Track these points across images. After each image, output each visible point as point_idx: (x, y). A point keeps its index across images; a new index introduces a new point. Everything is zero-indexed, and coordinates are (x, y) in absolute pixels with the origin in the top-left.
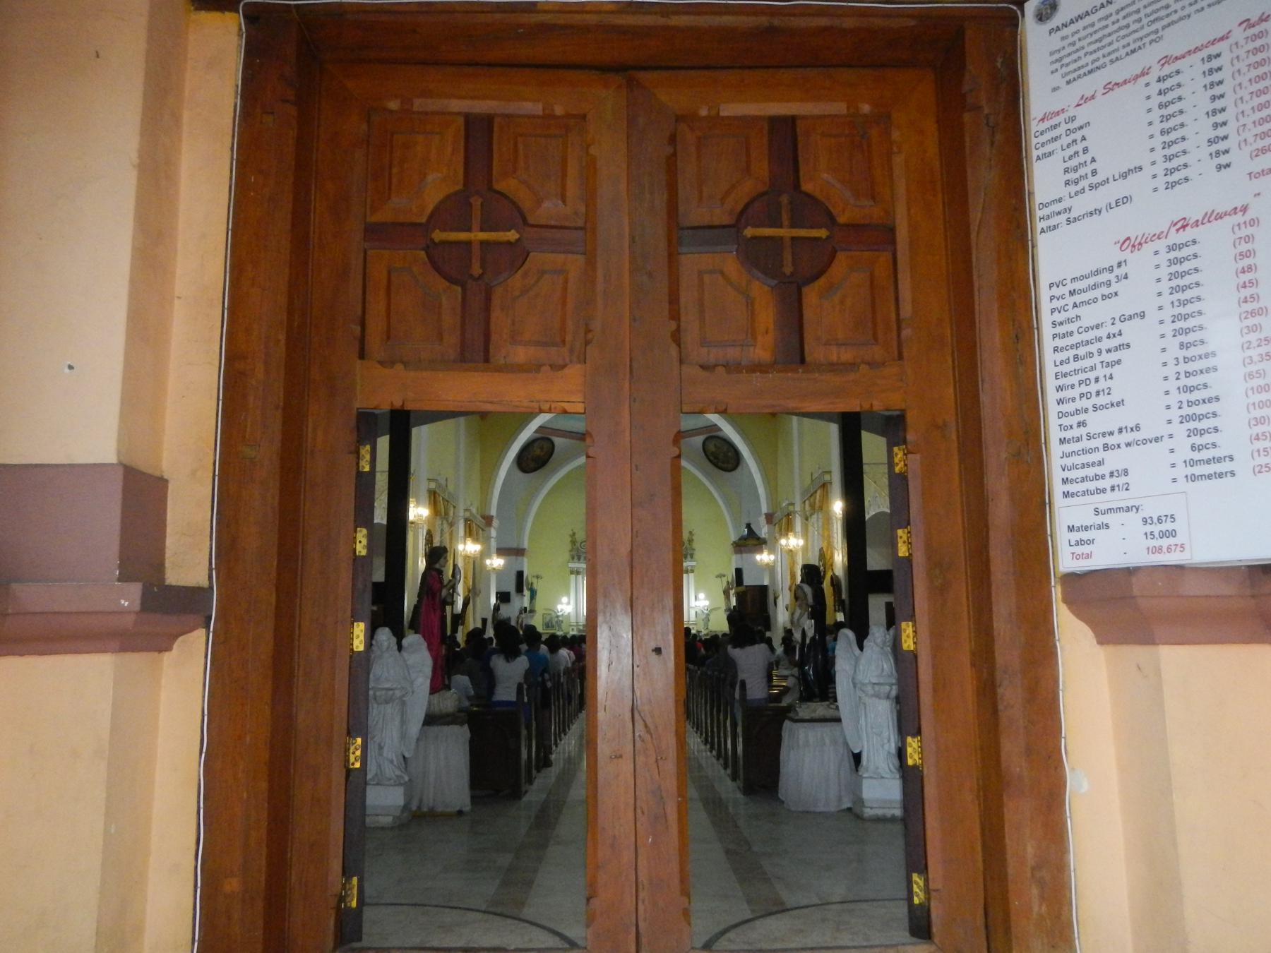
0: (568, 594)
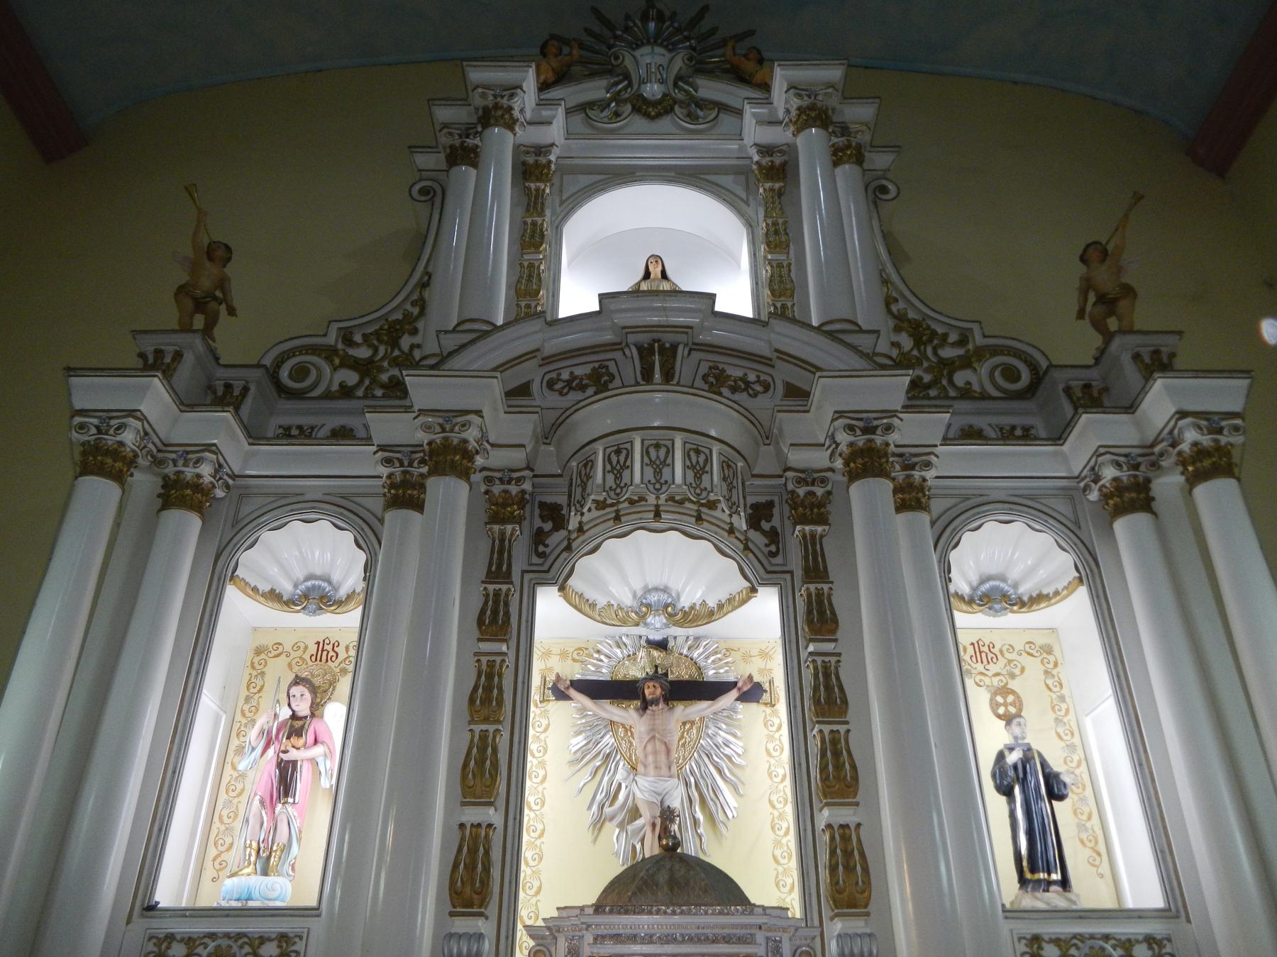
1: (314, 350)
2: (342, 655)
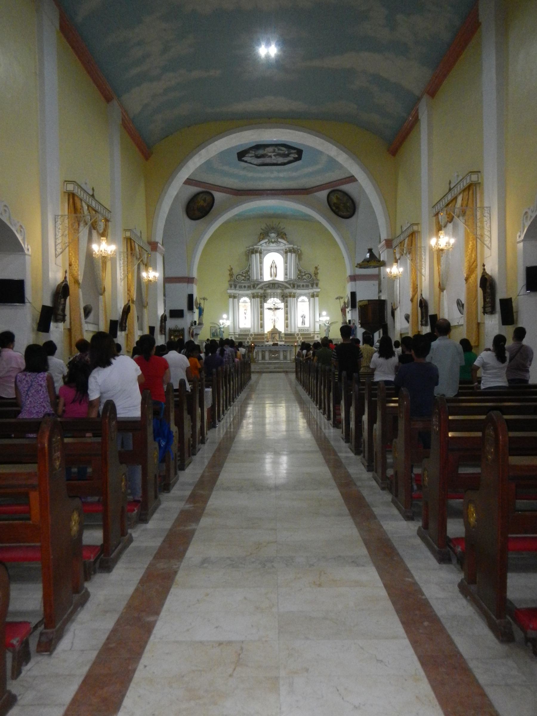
0: (228, 313)
1: (240, 275)
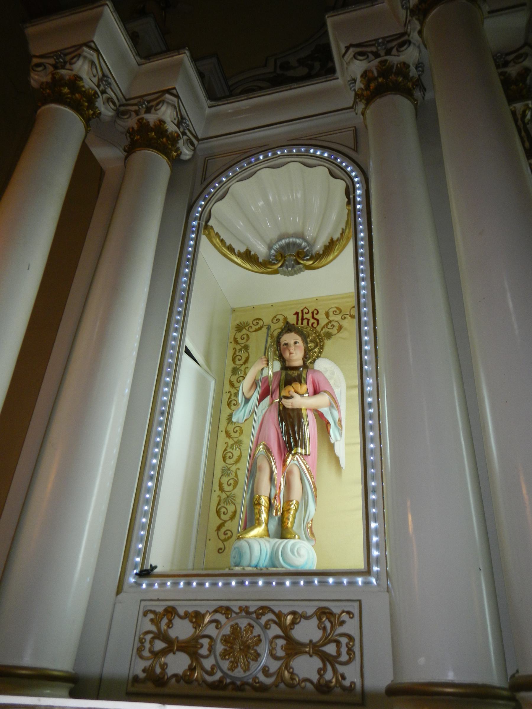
2: (323, 321)
